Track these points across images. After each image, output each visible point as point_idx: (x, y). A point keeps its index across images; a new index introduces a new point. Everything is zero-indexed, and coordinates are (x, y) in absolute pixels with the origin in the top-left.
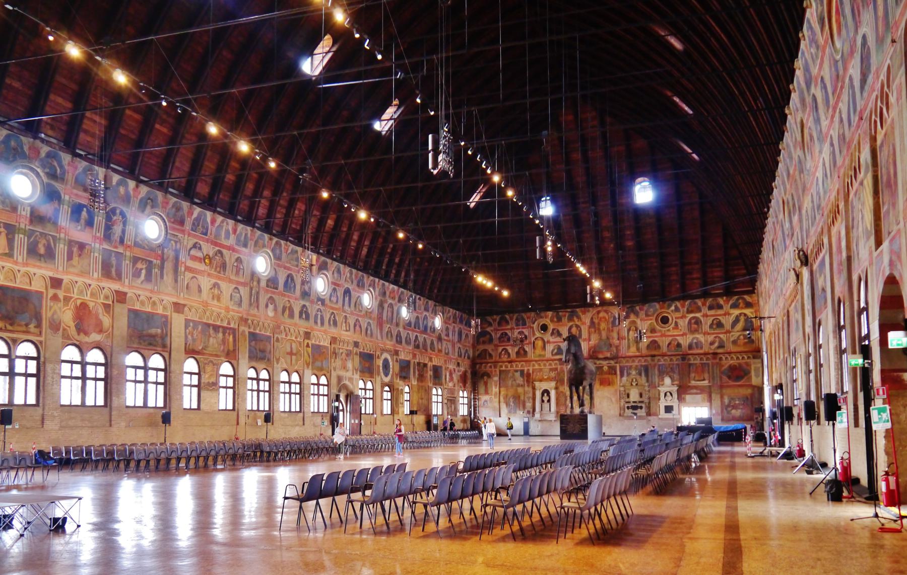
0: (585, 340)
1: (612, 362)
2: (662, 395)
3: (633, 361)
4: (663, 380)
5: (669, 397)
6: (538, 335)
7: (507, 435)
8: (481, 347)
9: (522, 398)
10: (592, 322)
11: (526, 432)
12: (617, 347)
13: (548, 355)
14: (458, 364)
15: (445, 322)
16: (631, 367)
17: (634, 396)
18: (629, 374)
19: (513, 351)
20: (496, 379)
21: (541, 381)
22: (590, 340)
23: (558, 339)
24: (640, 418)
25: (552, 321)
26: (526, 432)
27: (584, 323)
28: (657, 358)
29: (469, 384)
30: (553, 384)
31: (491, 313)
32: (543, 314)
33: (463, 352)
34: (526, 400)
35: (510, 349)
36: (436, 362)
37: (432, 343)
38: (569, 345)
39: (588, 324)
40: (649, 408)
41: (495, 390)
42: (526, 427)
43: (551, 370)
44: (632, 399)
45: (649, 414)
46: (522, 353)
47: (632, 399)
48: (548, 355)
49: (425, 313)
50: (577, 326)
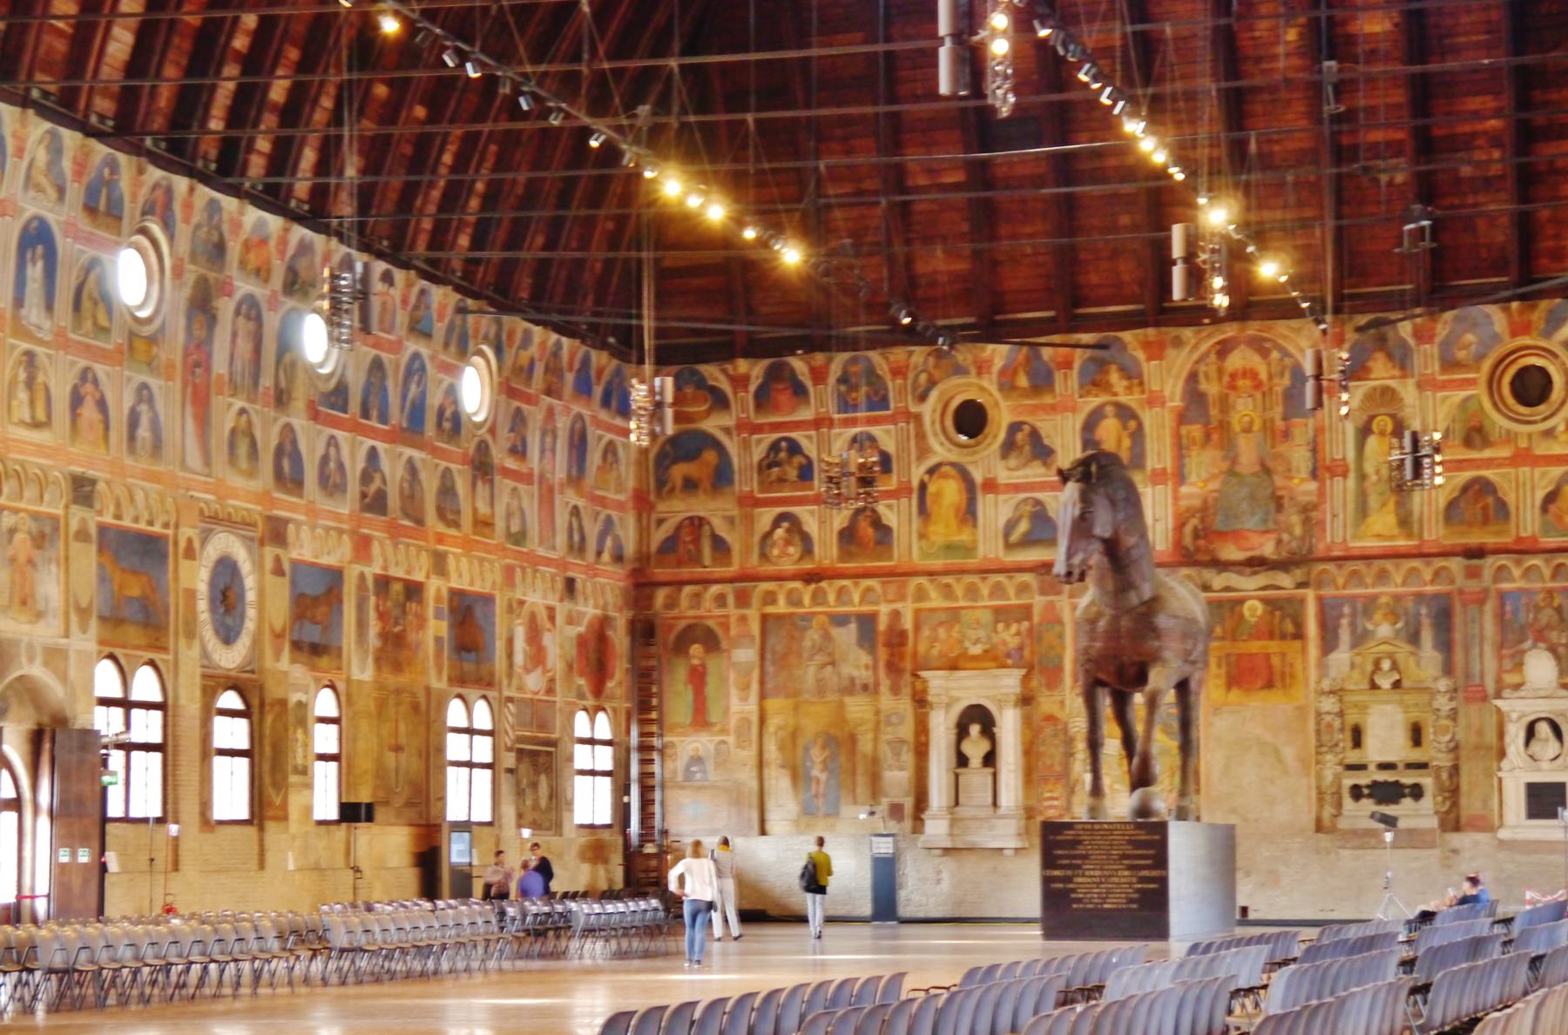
0: (1158, 477)
1: (1285, 580)
2: (1515, 734)
3: (1383, 576)
4: (1519, 666)
5: (1546, 745)
6: (941, 451)
7: (802, 920)
8: (677, 509)
9: (865, 745)
10: (1194, 396)
11: (885, 907)
12: (1306, 510)
13: (989, 547)
14: (570, 584)
15: (509, 387)
16: (1370, 604)
17: (1386, 739)
18: (1360, 638)
19: (823, 525)
20: (746, 655)
21: (953, 667)
22: (1180, 477)
23: (1036, 472)
24: (1413, 839)
25: (1007, 384)
26: (885, 907)
27: (1155, 400)
28: (1490, 564)
29: (619, 682)
30: (1010, 681)
31: (725, 350)
32: (964, 354)
33: (592, 530)
34: (885, 751)
35: (809, 517)
36: (465, 574)
37: (447, 490)
38: (1085, 499)
39: (1177, 403)
40: (1453, 793)
41: (739, 705)
42: (886, 877)
43: (1001, 614)
44: (1374, 751)
45: (1452, 822)
46: (867, 535)
47: (1374, 751)
48: (989, 547)
49: (412, 346)
50: (1125, 413)
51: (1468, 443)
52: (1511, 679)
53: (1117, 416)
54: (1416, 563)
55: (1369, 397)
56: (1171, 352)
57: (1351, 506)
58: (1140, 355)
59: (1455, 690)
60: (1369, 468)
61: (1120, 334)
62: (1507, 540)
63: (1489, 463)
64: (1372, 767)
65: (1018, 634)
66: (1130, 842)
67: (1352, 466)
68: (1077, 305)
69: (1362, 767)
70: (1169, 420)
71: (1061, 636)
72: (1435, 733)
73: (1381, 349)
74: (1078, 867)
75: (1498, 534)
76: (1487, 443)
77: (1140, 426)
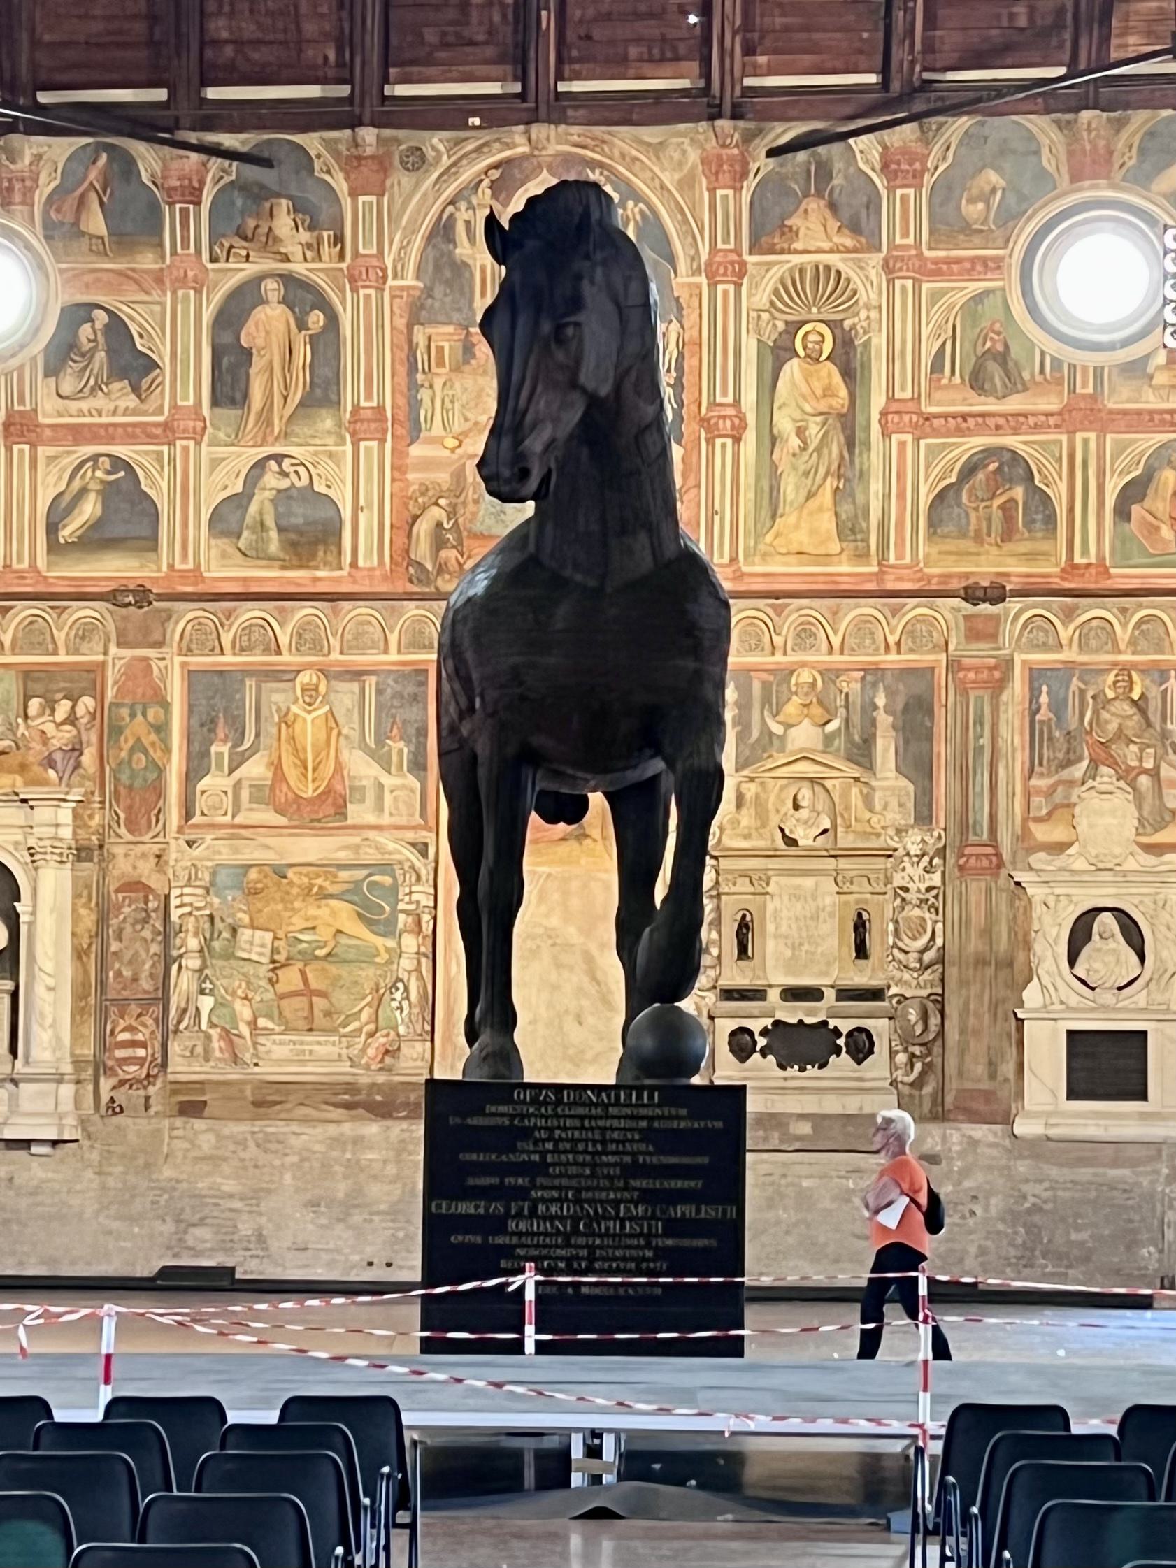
0: (362, 426)
4: (1063, 809)
23: (116, 404)
50: (301, 296)
51: (977, 382)
52: (1041, 833)
53: (284, 301)
54: (867, 608)
55: (791, 286)
56: (401, 180)
57: (747, 497)
58: (340, 183)
59: (942, 853)
60: (784, 423)
61: (298, 138)
62: (1049, 570)
63: (1016, 421)
64: (774, 995)
65: (71, 720)
66: (647, 1135)
67: (751, 419)
68: (205, 83)
69: (757, 994)
70: (393, 317)
71: (161, 729)
72: (897, 933)
73: (819, 194)
74: (522, 1193)
75: (1031, 556)
76: (1014, 384)
77: (333, 320)
